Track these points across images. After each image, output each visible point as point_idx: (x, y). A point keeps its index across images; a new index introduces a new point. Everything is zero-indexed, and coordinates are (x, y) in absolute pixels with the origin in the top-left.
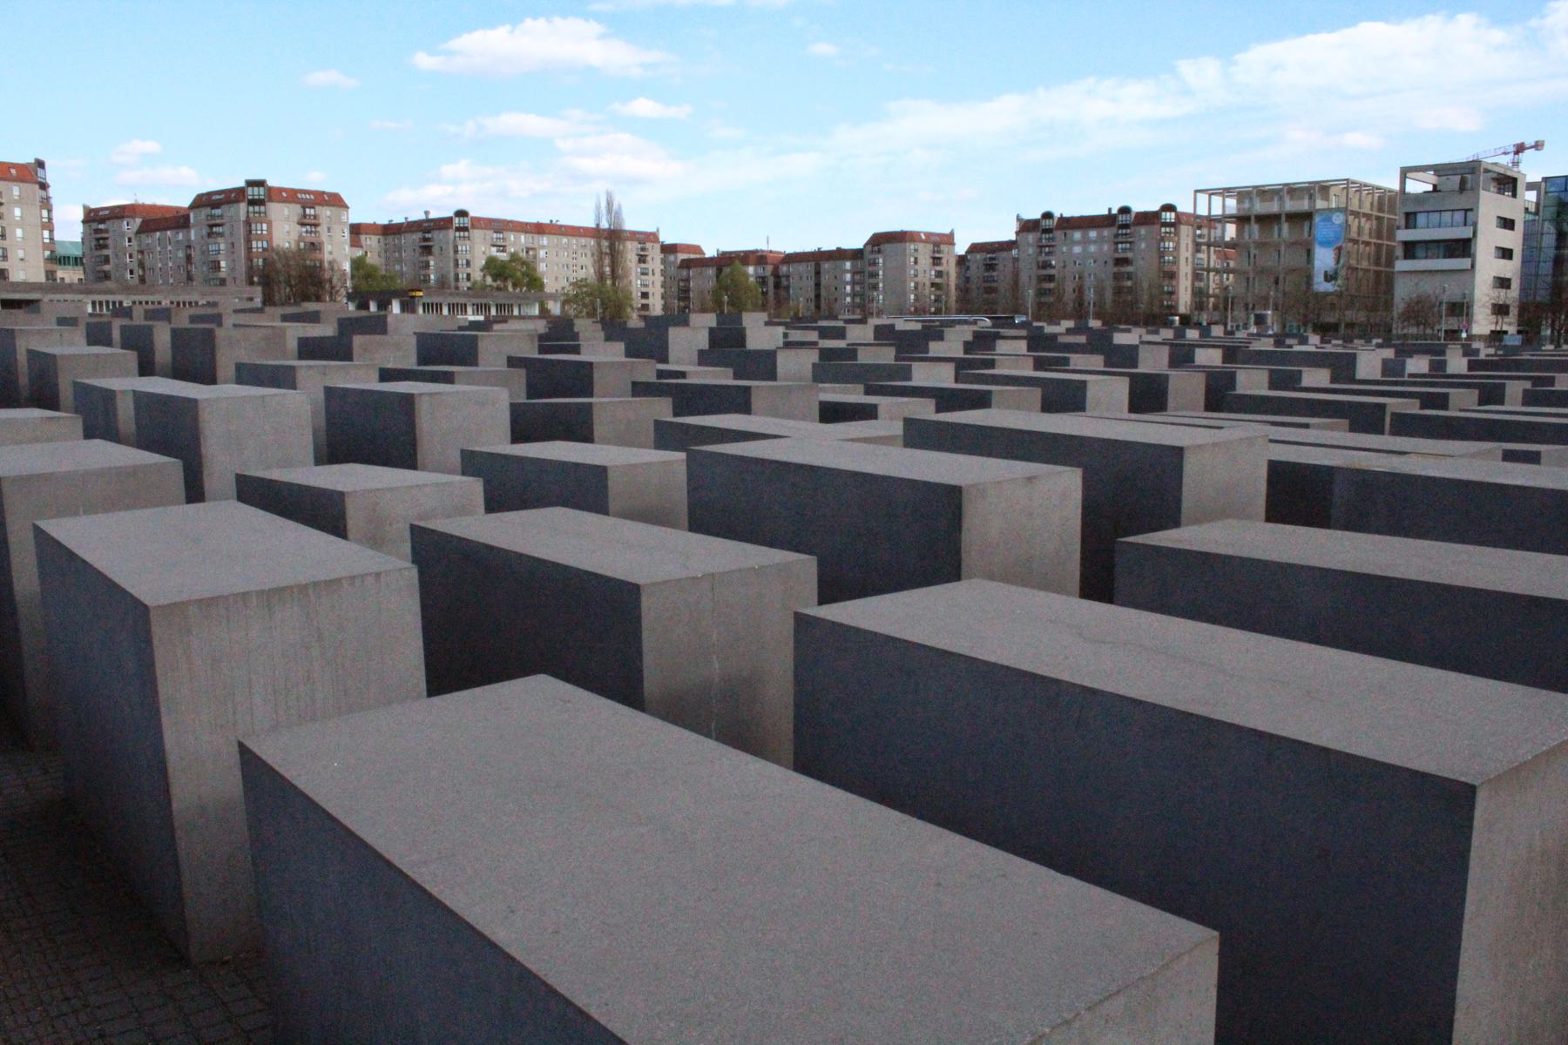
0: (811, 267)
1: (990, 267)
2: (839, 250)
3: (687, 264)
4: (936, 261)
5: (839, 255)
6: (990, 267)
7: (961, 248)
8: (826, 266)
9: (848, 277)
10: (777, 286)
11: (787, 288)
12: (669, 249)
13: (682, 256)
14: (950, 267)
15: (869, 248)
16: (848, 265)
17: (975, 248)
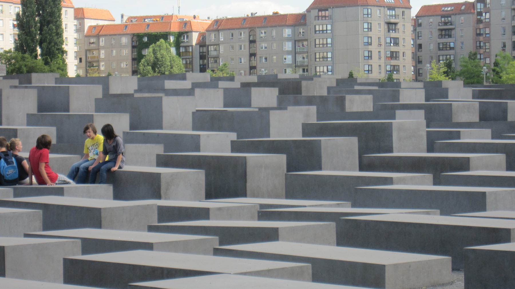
0: (244, 35)
1: (446, 32)
2: (276, 14)
3: (98, 33)
4: (391, 26)
5: (276, 20)
6: (446, 32)
7: (414, 12)
8: (262, 34)
9: (288, 46)
10: (203, 57)
11: (216, 59)
12: (80, 15)
13: (88, 23)
14: (406, 35)
15: (315, 13)
16: (287, 32)
17: (427, 11)
